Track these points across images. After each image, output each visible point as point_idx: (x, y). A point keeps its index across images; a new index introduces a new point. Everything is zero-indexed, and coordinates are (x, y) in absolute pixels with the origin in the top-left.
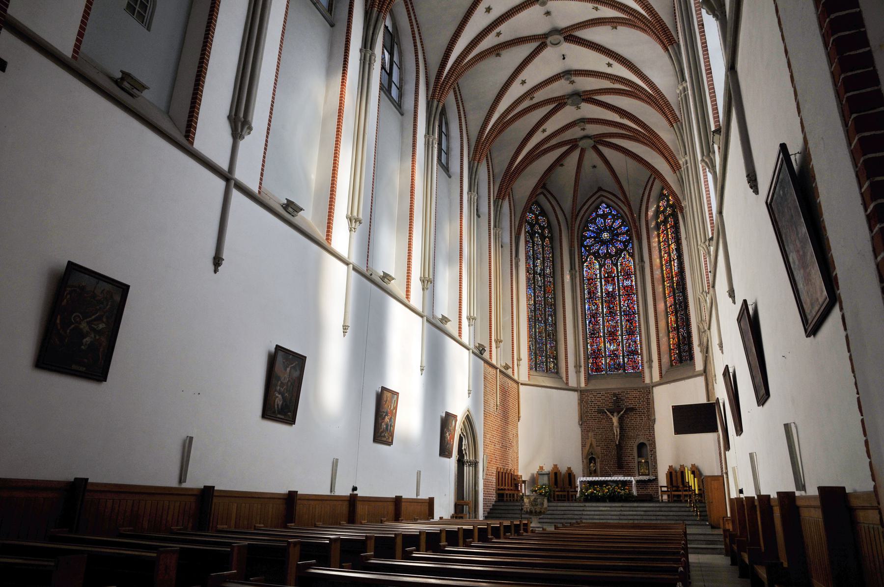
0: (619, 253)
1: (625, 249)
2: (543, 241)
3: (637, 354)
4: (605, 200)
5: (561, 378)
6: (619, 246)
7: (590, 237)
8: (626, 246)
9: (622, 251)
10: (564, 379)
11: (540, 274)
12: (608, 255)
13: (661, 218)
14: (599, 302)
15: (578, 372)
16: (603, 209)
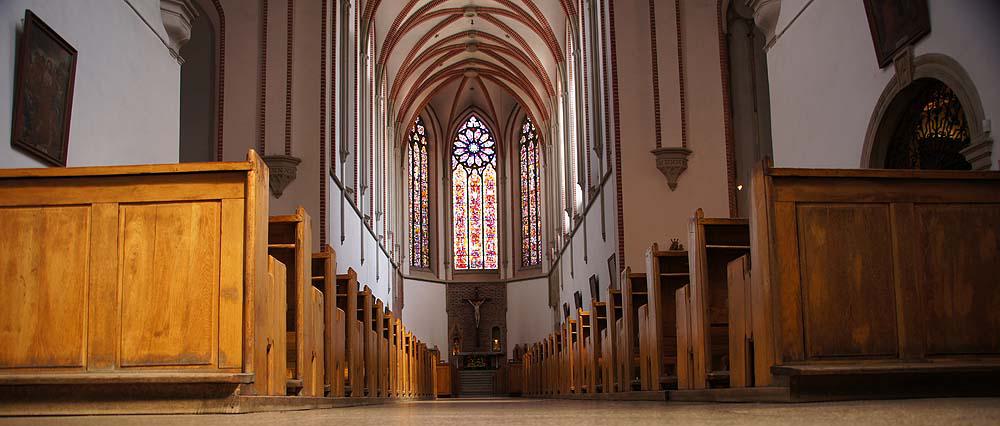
0: (484, 164)
2: (421, 149)
6: (486, 159)
8: (491, 160)
9: (487, 163)
12: (474, 166)
14: (465, 208)
15: (446, 268)
16: (473, 122)
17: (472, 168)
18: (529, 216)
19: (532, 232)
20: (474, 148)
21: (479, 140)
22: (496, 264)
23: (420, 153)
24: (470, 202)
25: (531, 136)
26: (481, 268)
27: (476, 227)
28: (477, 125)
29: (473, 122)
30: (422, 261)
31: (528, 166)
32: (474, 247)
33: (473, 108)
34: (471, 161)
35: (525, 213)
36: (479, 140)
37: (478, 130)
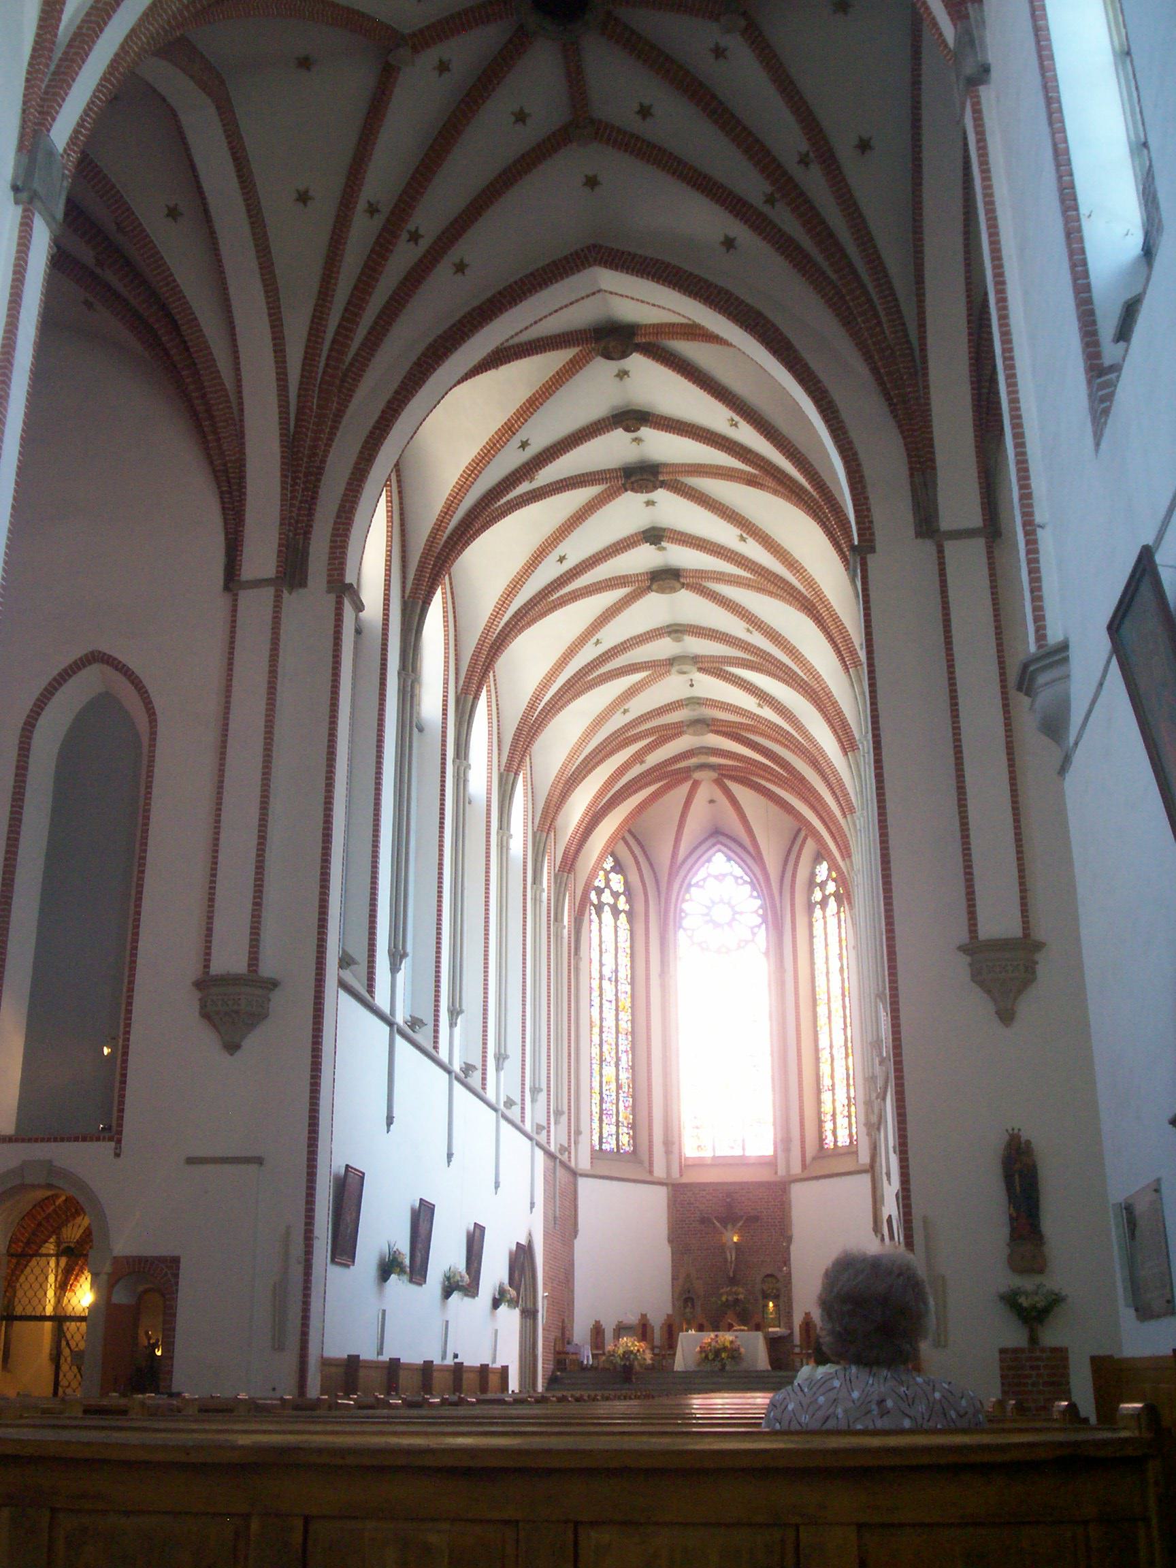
5: (641, 1162)
10: (646, 1164)
11: (610, 979)
23: (616, 927)
30: (617, 1140)
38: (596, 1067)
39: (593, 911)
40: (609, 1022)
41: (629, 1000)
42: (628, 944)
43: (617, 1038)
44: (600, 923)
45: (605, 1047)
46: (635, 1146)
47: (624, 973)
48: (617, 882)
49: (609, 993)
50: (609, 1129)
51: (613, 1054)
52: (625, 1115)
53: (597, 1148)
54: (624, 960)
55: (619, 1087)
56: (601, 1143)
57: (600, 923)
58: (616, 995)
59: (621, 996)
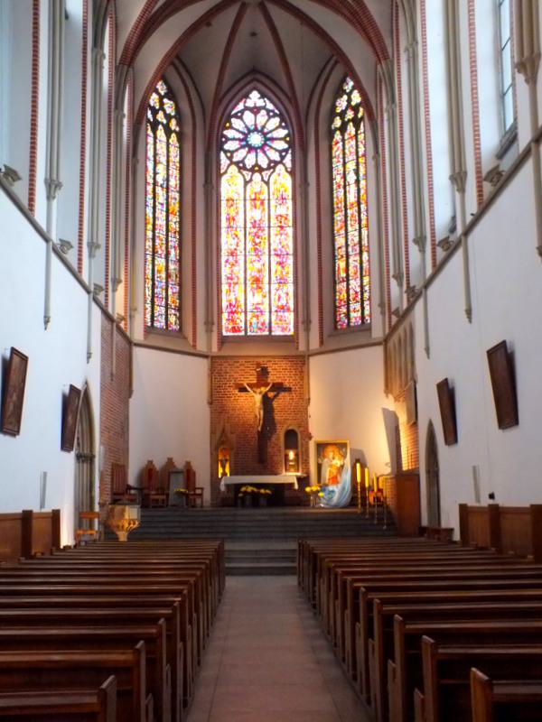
0: (273, 165)
1: (281, 162)
2: (168, 137)
3: (288, 310)
4: (259, 86)
5: (185, 338)
6: (276, 157)
7: (234, 139)
8: (283, 158)
9: (276, 163)
11: (162, 186)
12: (257, 169)
13: (338, 122)
14: (241, 235)
15: (209, 331)
16: (255, 98)
17: (252, 170)
18: (347, 245)
19: (351, 271)
20: (256, 139)
21: (264, 127)
22: (291, 326)
23: (168, 144)
24: (249, 225)
25: (350, 115)
26: (266, 333)
27: (258, 265)
28: (260, 103)
29: (255, 98)
31: (344, 164)
32: (254, 299)
33: (255, 76)
34: (250, 162)
35: (340, 241)
36: (264, 127)
37: (263, 112)
38: (149, 258)
39: (149, 128)
40: (161, 222)
41: (177, 205)
42: (178, 159)
43: (167, 235)
44: (155, 138)
45: (158, 241)
46: (181, 325)
47: (174, 182)
48: (169, 106)
49: (161, 198)
50: (160, 310)
51: (164, 248)
52: (173, 300)
53: (149, 324)
54: (174, 172)
55: (168, 276)
56: (152, 320)
57: (155, 138)
58: (167, 199)
59: (172, 202)
